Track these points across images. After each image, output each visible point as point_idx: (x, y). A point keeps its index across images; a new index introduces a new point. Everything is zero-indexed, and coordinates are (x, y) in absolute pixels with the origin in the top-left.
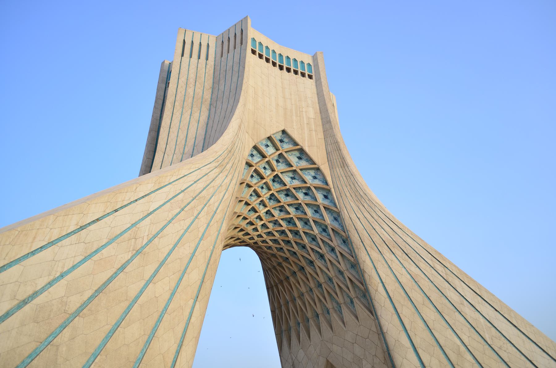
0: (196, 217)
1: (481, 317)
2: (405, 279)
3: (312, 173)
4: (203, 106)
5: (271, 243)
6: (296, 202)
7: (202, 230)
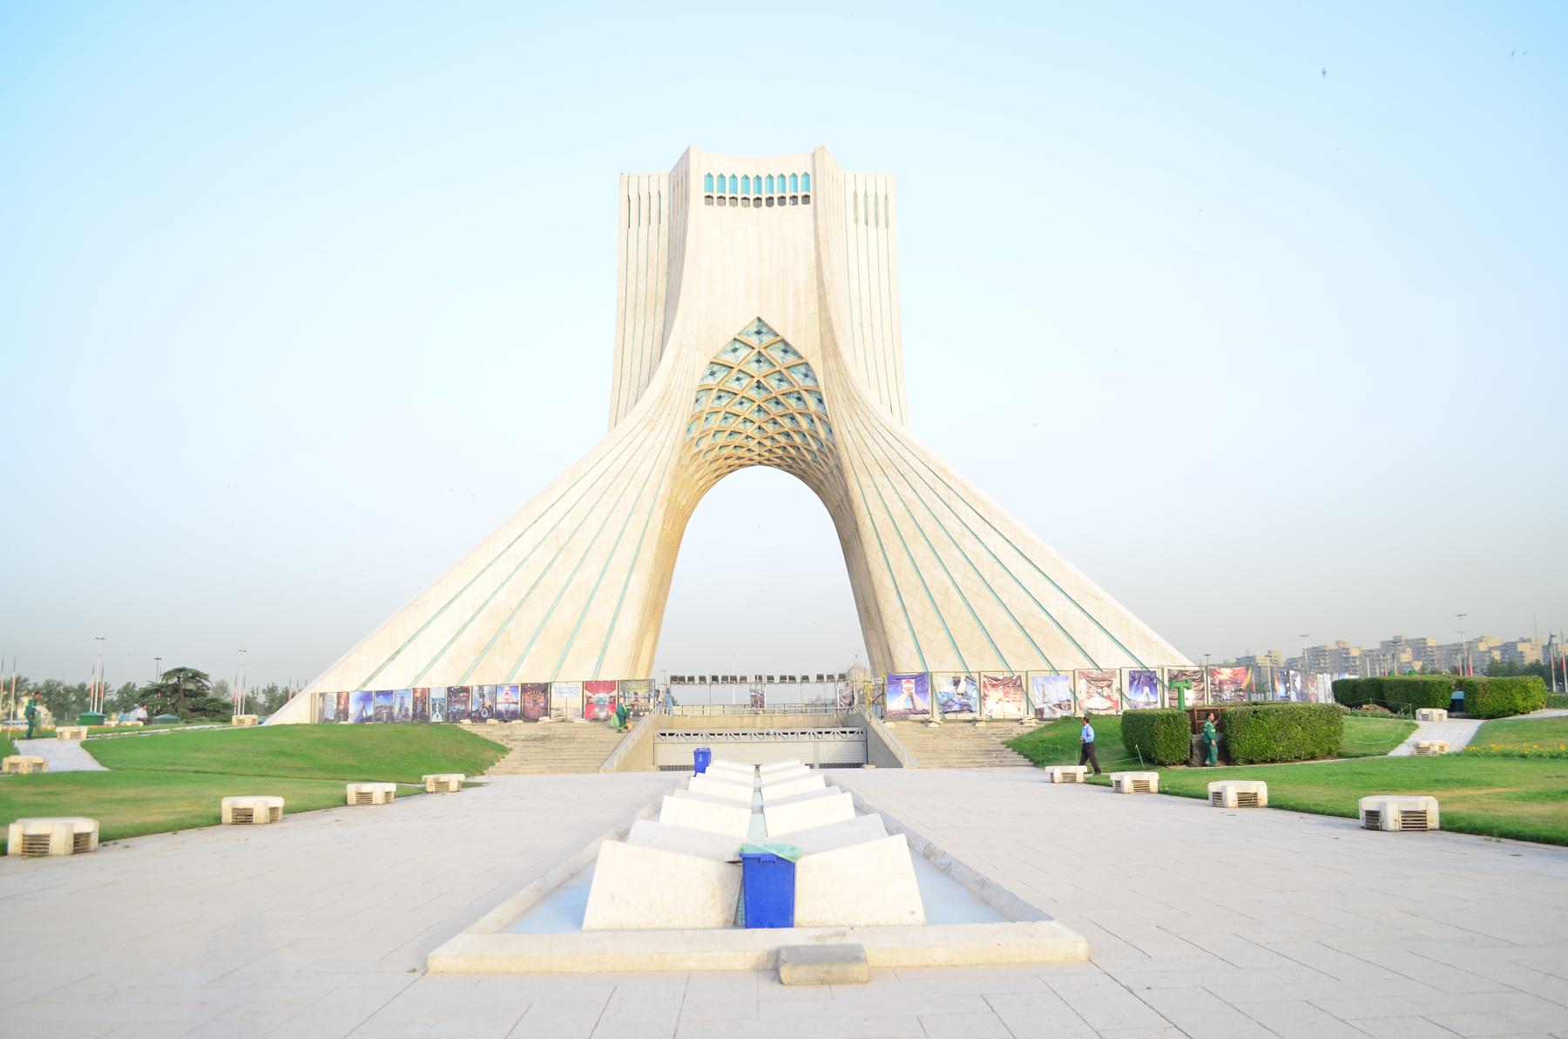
2: (897, 509)
3: (803, 369)
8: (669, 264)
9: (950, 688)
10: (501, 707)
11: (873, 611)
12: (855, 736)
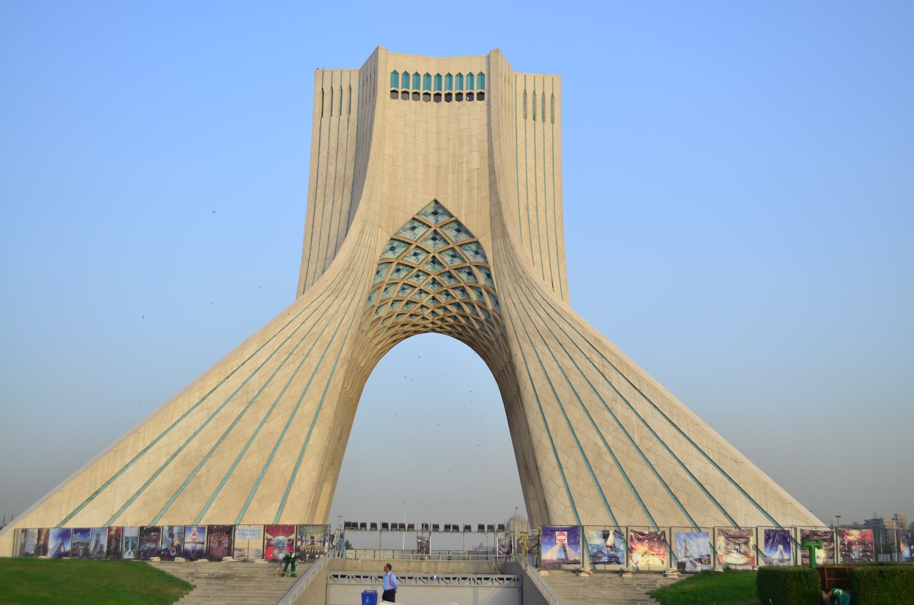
0: (307, 355)
1: (634, 414)
2: (555, 374)
3: (474, 247)
4: (346, 188)
5: (449, 329)
6: (458, 285)
7: (315, 365)
8: (357, 150)
9: (599, 541)
10: (188, 546)
11: (532, 468)
12: (513, 584)
